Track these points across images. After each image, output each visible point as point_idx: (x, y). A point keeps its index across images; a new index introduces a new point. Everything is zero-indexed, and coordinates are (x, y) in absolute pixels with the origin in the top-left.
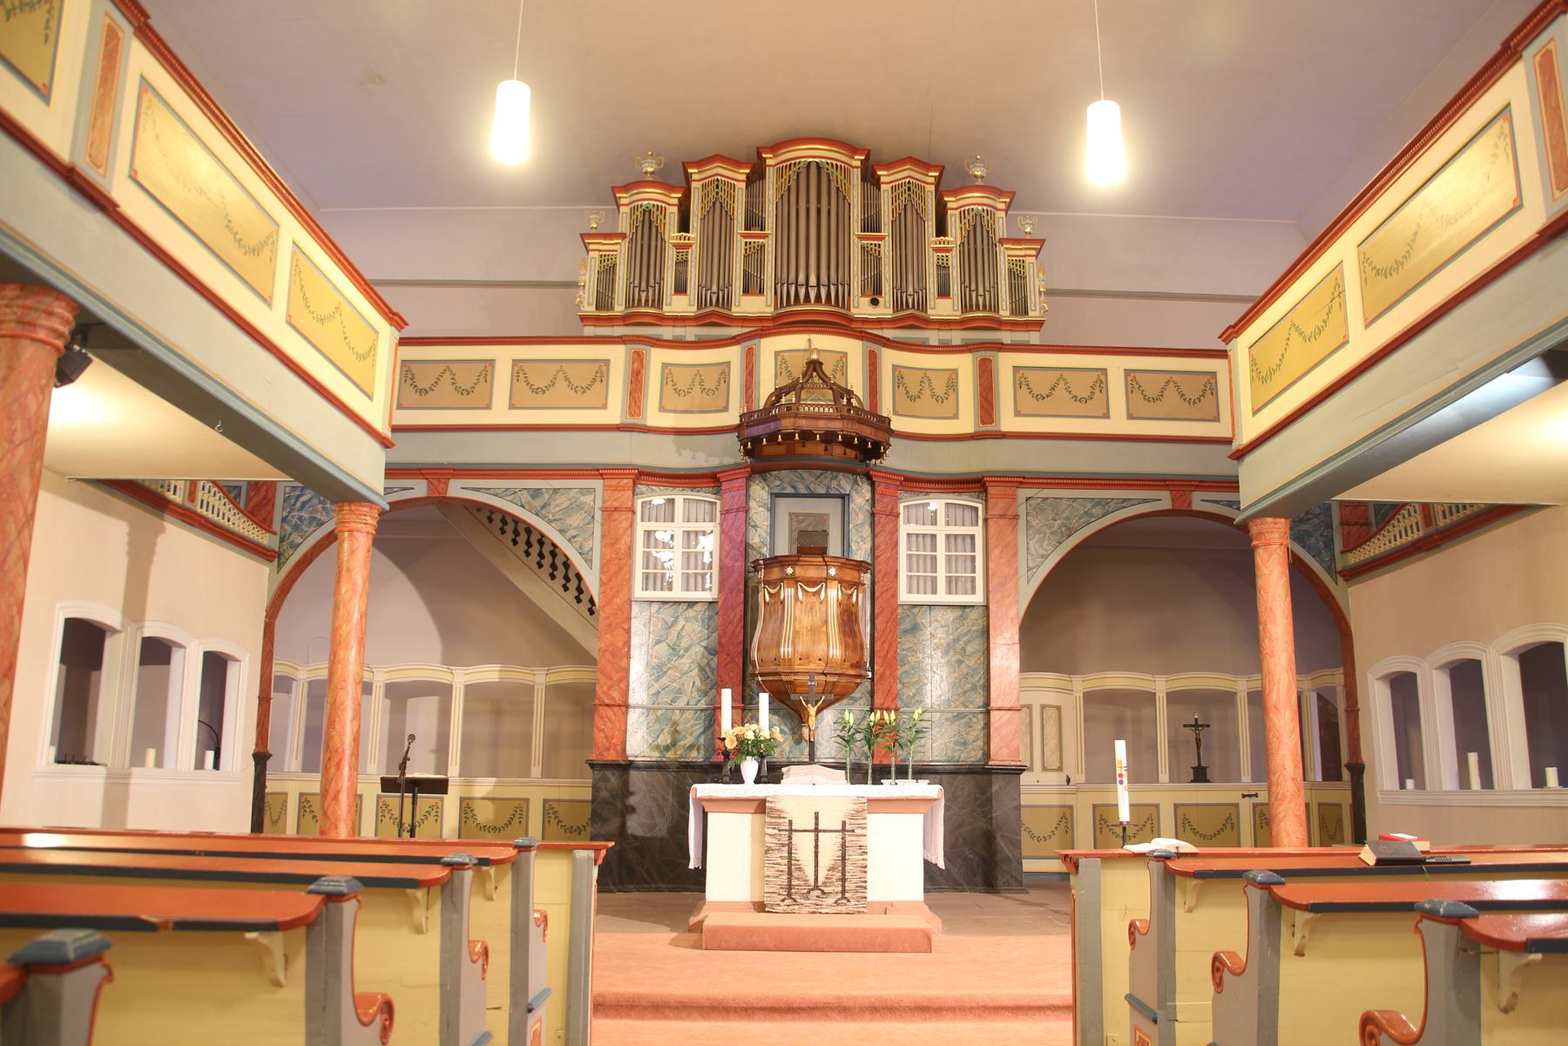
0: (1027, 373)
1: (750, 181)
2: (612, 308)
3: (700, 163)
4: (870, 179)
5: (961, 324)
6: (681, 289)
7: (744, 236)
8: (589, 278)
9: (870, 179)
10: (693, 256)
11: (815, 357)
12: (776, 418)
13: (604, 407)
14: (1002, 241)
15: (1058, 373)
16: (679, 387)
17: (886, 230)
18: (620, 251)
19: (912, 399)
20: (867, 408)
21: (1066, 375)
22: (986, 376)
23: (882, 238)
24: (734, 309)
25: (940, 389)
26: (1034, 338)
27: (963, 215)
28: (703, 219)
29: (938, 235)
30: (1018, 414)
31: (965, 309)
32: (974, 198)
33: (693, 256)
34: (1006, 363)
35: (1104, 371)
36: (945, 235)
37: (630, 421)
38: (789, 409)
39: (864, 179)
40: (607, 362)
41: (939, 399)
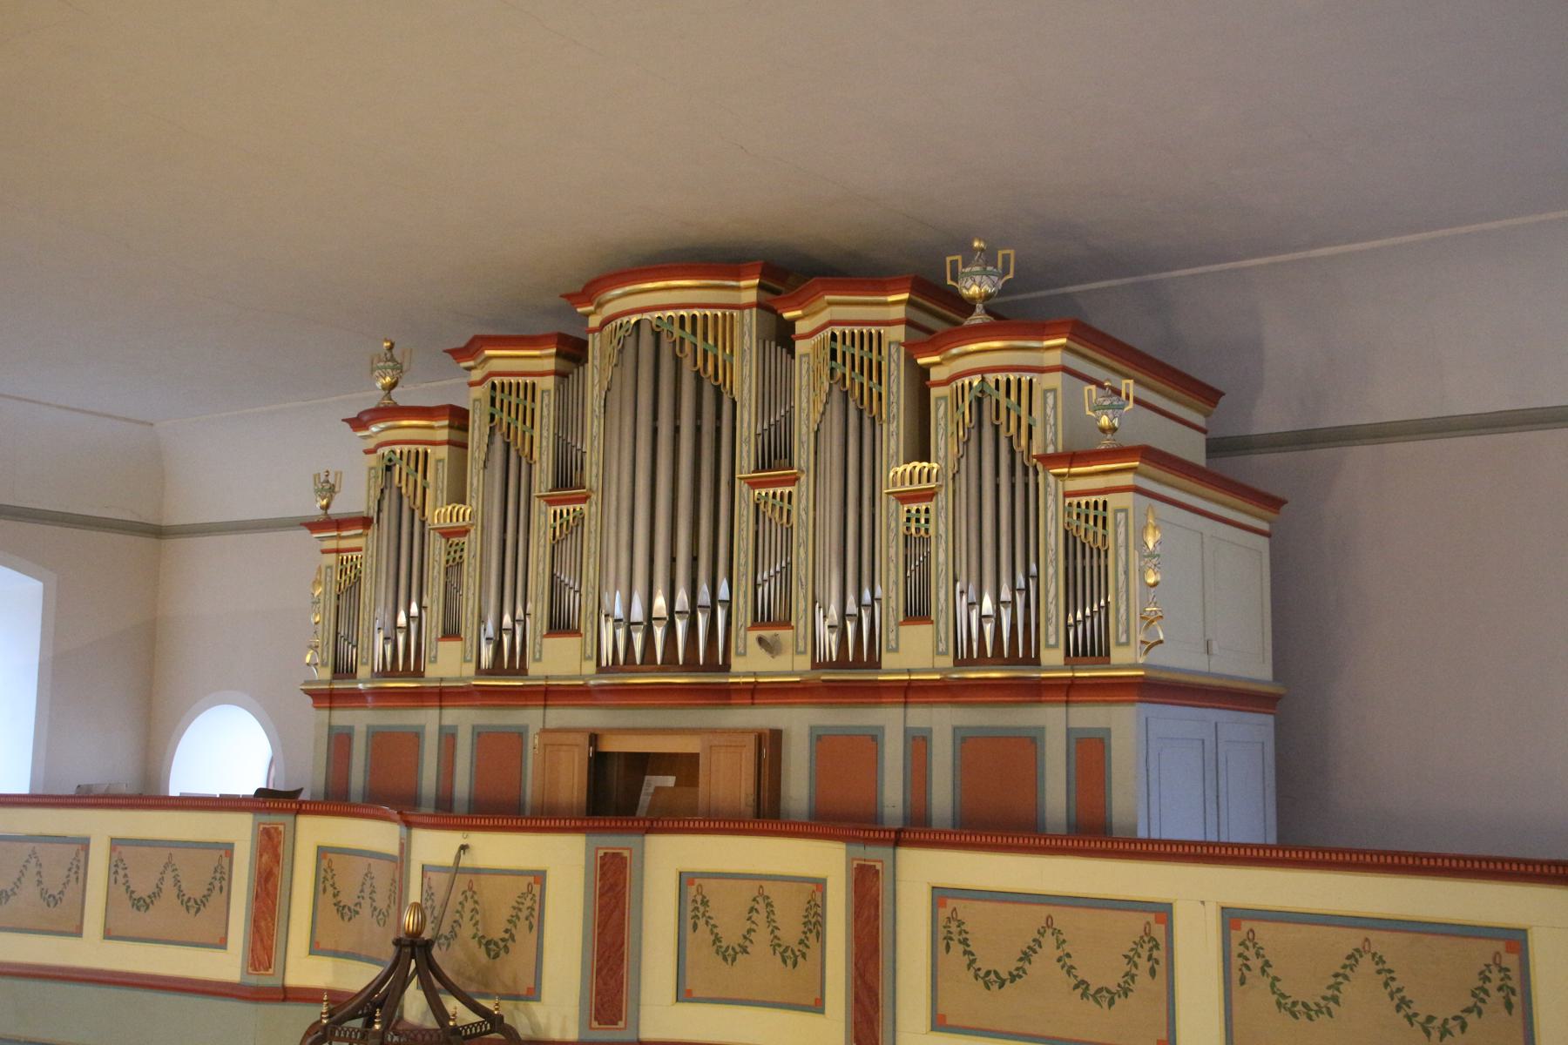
0: (966, 910)
7: (551, 502)
14: (1049, 460)
15: (1044, 911)
19: (728, 955)
21: (1062, 917)
25: (791, 931)
35: (1163, 912)
37: (254, 980)
41: (790, 956)
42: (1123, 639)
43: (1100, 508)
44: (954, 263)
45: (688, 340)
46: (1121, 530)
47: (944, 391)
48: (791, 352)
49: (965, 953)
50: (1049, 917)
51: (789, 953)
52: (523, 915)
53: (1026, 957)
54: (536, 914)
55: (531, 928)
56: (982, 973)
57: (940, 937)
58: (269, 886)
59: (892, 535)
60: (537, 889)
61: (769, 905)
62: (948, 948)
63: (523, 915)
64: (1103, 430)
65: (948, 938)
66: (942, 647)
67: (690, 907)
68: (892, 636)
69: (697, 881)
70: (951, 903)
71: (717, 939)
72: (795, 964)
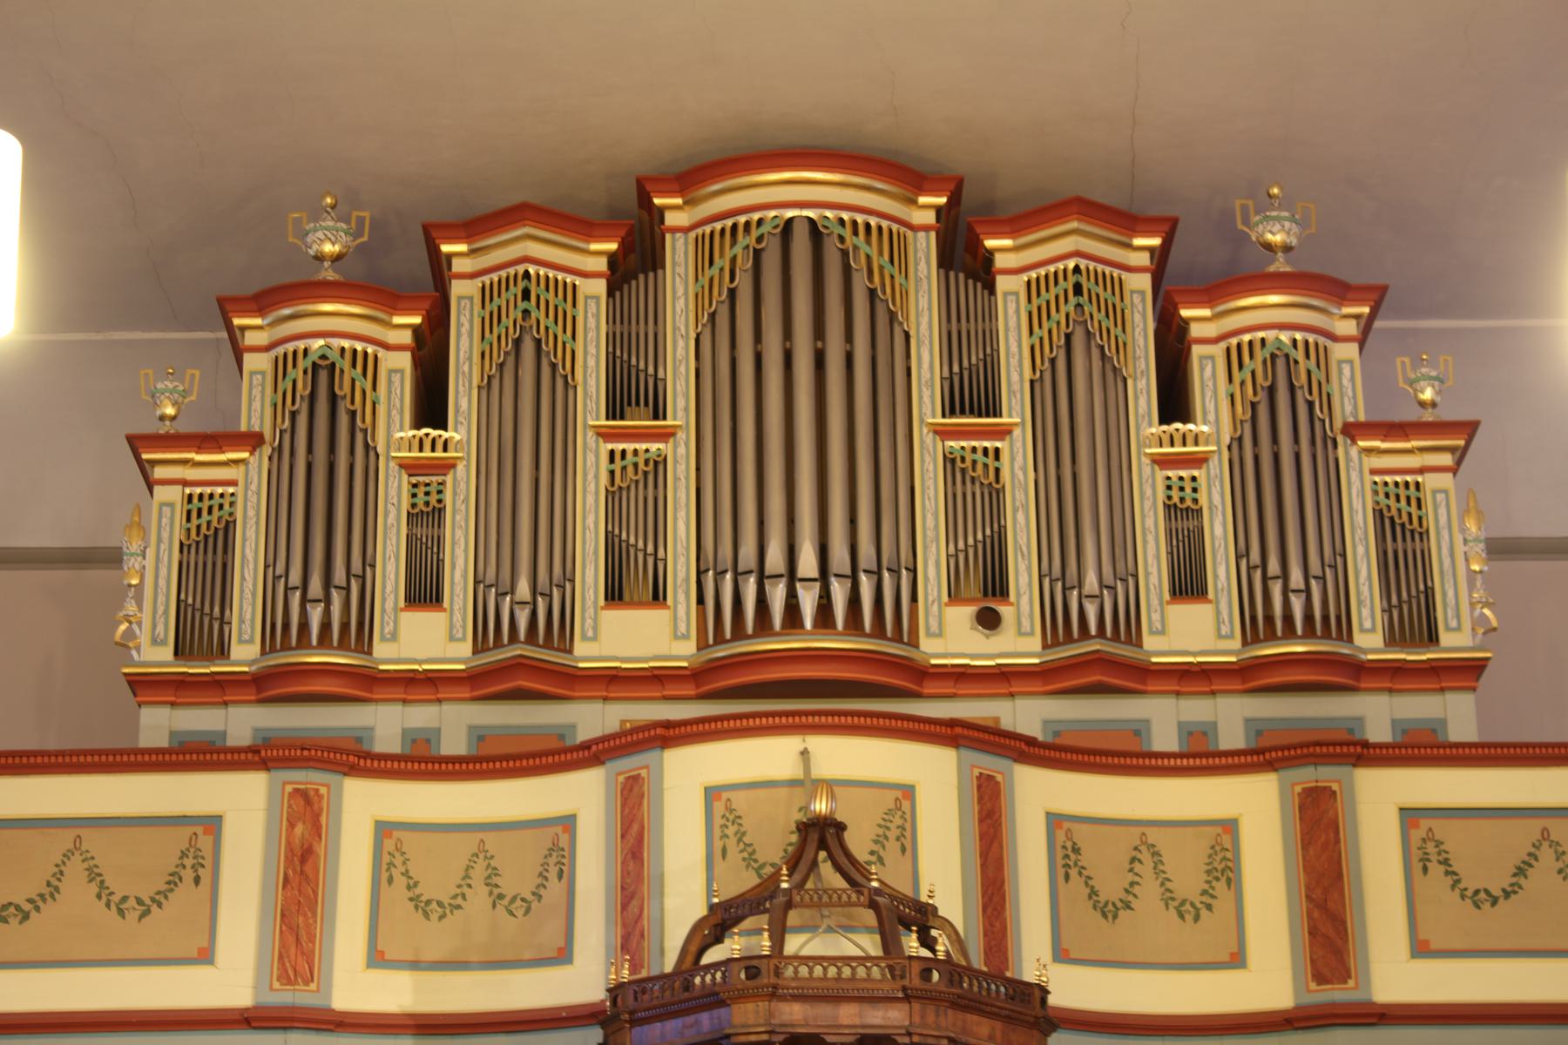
0: (1440, 828)
1: (620, 275)
2: (223, 652)
3: (475, 227)
4: (965, 260)
5: (1244, 676)
6: (424, 591)
7: (606, 435)
8: (154, 571)
9: (965, 260)
10: (460, 495)
11: (821, 806)
12: (714, 1000)
13: (205, 956)
14: (1353, 430)
15: (1536, 825)
16: (426, 891)
17: (1015, 410)
18: (244, 480)
19: (1108, 911)
20: (978, 962)
22: (1321, 839)
23: (1003, 432)
24: (580, 648)
25: (1188, 882)
26: (1459, 716)
27: (1235, 359)
28: (486, 386)
29: (1165, 418)
30: (1421, 949)
31: (1251, 636)
32: (1265, 310)
33: (460, 495)
34: (1379, 798)
36: (1186, 418)
38: (753, 972)
39: (946, 261)
40: (212, 824)
42: (1454, 624)
43: (1412, 488)
44: (1245, 209)
45: (864, 248)
46: (1442, 511)
47: (1218, 350)
48: (990, 287)
49: (1447, 873)
50: (1545, 829)
51: (1188, 906)
52: (892, 834)
53: (1520, 872)
54: (908, 834)
55: (904, 850)
56: (1469, 893)
57: (1415, 860)
58: (308, 868)
59: (1148, 504)
60: (906, 805)
61: (1156, 854)
62: (1425, 869)
63: (892, 834)
64: (1422, 404)
65: (1425, 860)
66: (1225, 630)
67: (1060, 853)
68: (1156, 617)
69: (1066, 825)
70: (1425, 824)
71: (1093, 893)
72: (1197, 918)
